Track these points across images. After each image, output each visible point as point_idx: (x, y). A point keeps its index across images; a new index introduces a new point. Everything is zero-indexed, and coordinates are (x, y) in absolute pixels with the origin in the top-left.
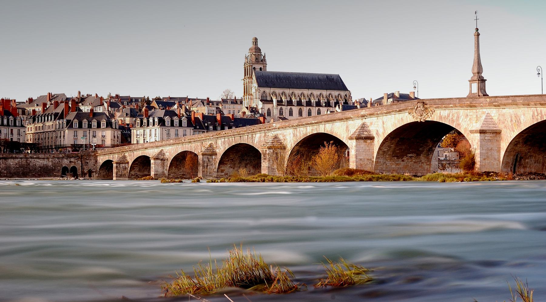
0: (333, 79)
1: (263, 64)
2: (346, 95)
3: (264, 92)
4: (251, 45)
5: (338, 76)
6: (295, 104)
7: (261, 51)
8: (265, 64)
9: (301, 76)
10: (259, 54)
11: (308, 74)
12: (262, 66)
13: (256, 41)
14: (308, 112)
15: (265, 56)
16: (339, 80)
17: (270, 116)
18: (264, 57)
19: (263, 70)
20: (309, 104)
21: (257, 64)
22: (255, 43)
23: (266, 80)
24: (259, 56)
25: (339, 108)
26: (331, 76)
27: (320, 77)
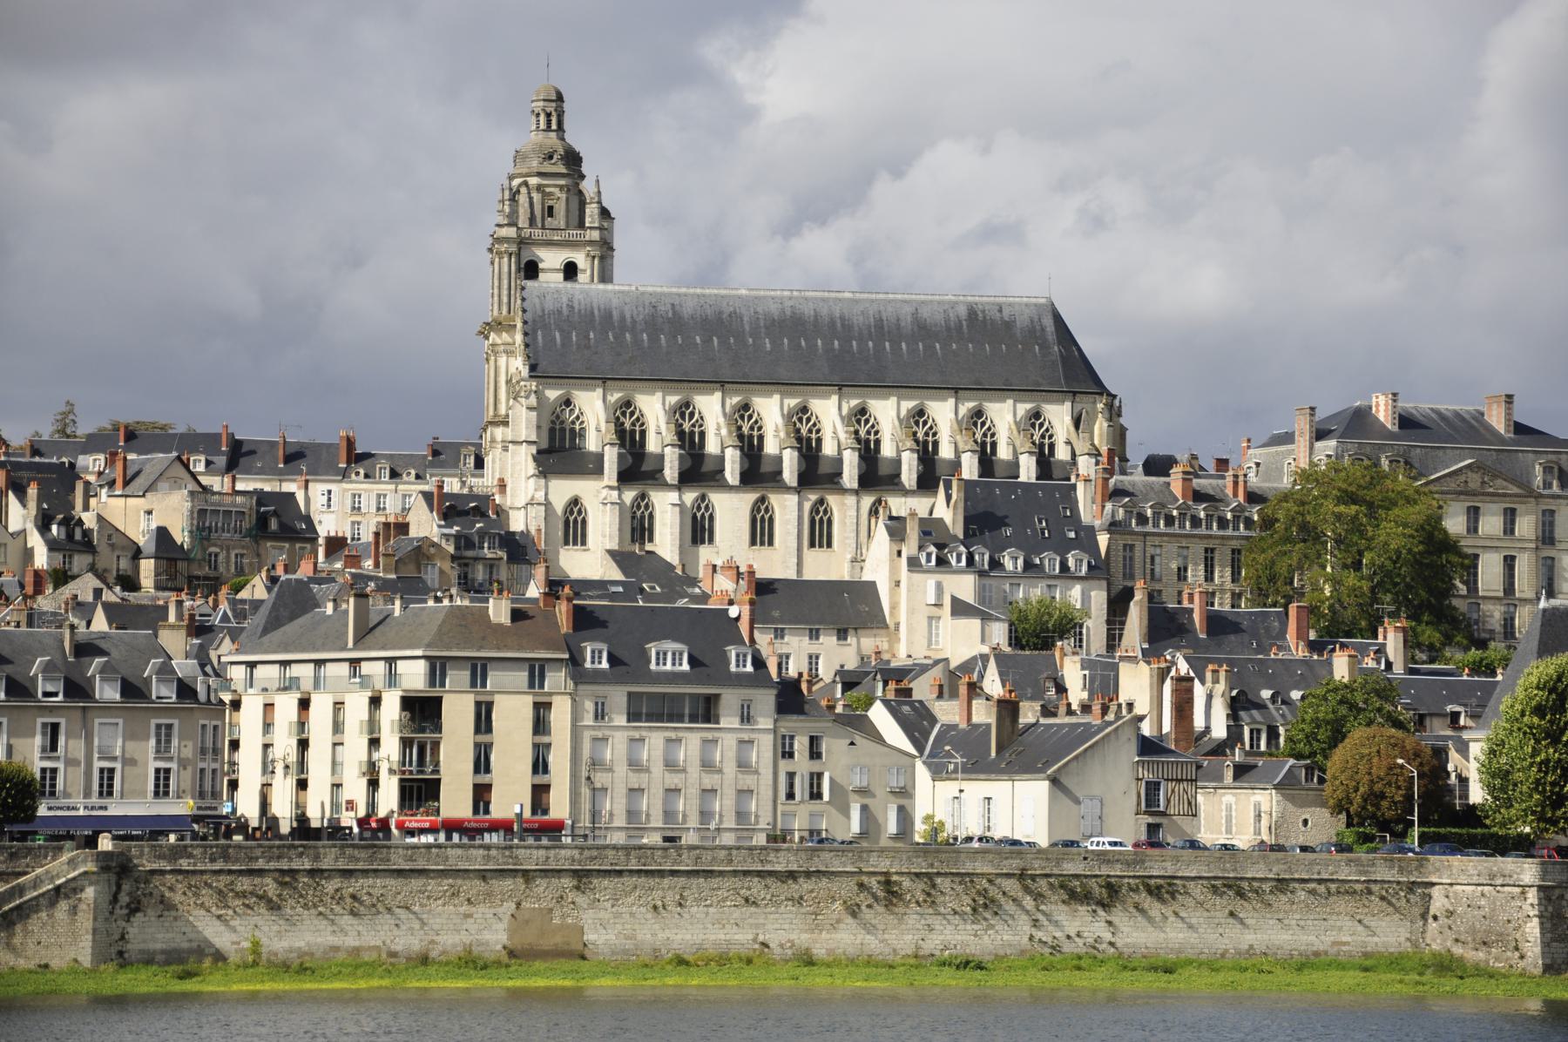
0: (1009, 325)
7: (585, 169)
9: (808, 310)
14: (812, 522)
16: (1043, 330)
17: (584, 543)
22: (542, 118)
25: (948, 498)
27: (925, 313)
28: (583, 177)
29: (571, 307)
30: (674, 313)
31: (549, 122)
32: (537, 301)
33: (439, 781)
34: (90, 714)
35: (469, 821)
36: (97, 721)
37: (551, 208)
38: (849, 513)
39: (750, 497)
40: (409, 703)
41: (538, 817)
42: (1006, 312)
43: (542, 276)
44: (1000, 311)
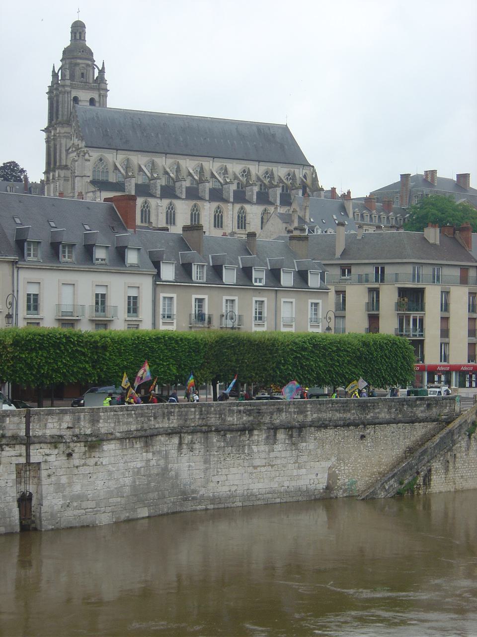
0: (273, 136)
1: (99, 89)
2: (305, 177)
3: (101, 160)
4: (67, 43)
5: (285, 129)
6: (181, 193)
8: (102, 89)
10: (90, 63)
11: (213, 121)
12: (95, 96)
13: (78, 29)
15: (103, 68)
18: (102, 72)
19: (97, 104)
20: (217, 195)
21: (83, 88)
23: (106, 131)
24: (89, 68)
26: (269, 126)
28: (94, 61)
29: (98, 117)
30: (141, 122)
31: (80, 36)
32: (83, 113)
33: (422, 342)
34: (279, 295)
35: (464, 366)
36: (283, 300)
37: (83, 74)
38: (229, 213)
39: (191, 203)
40: (402, 292)
41: (471, 363)
42: (272, 131)
43: (80, 103)
44: (269, 129)
